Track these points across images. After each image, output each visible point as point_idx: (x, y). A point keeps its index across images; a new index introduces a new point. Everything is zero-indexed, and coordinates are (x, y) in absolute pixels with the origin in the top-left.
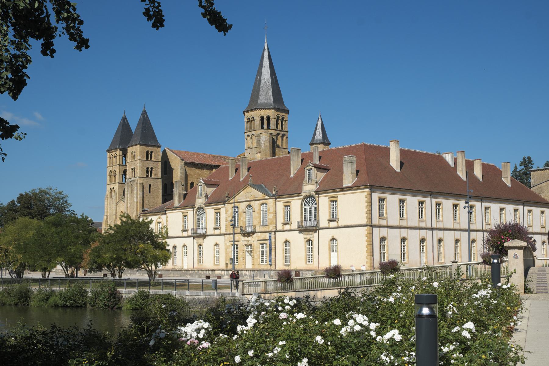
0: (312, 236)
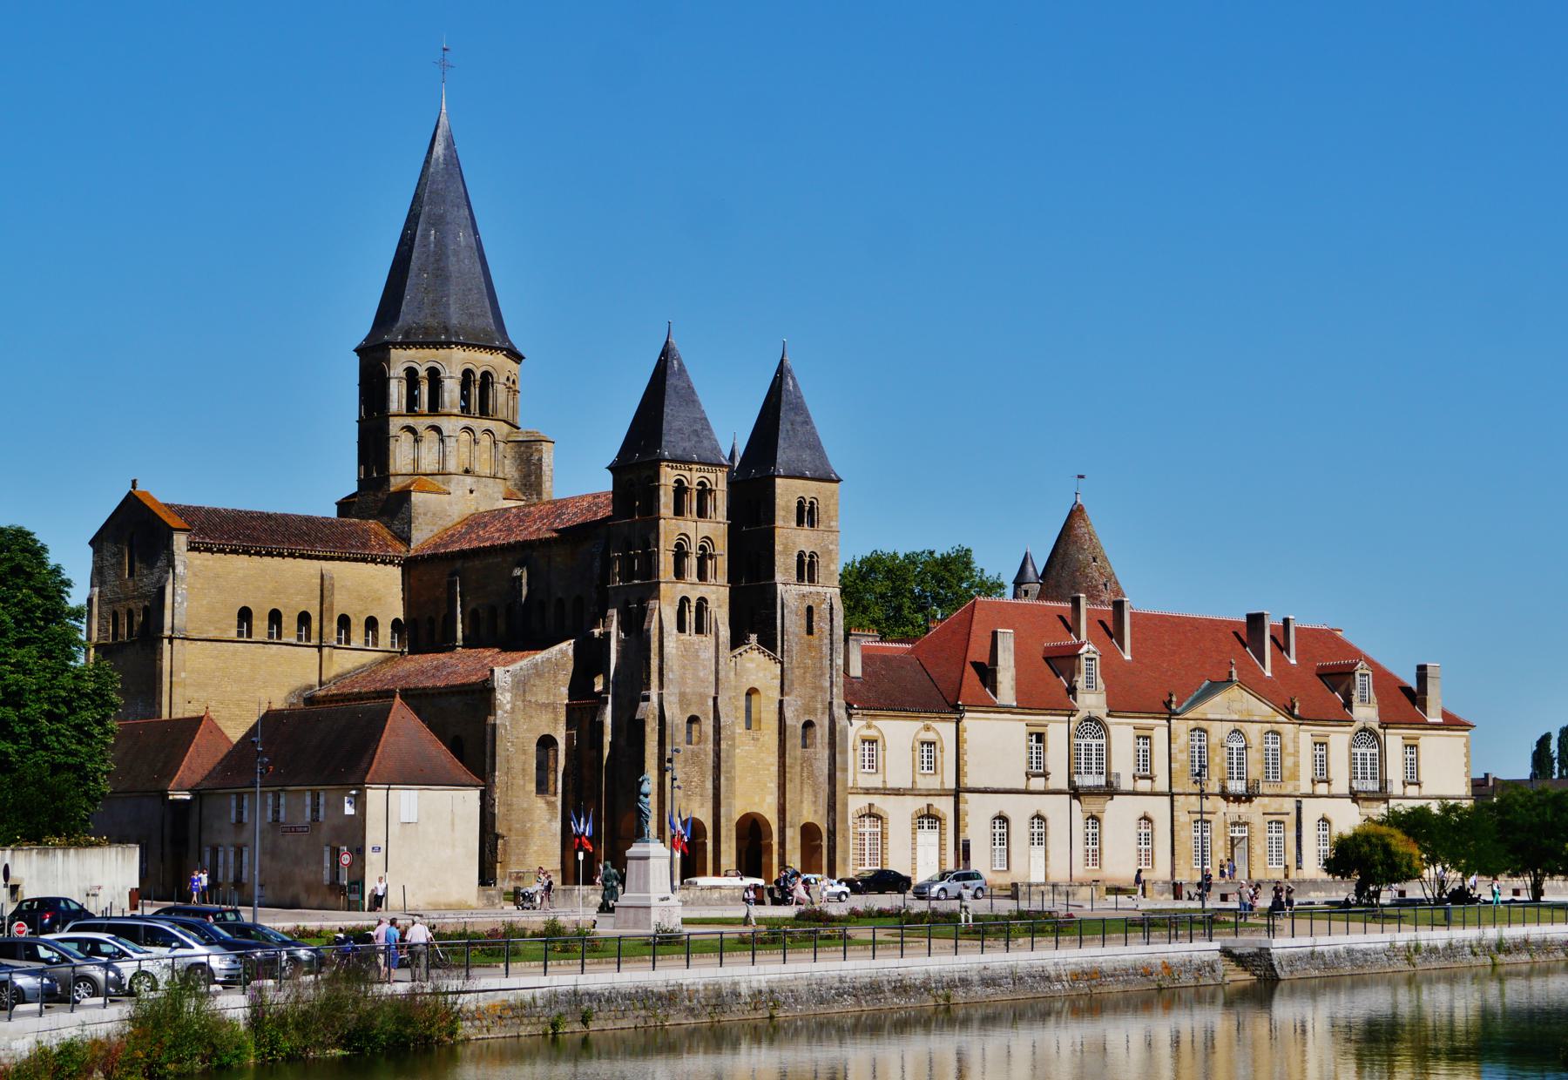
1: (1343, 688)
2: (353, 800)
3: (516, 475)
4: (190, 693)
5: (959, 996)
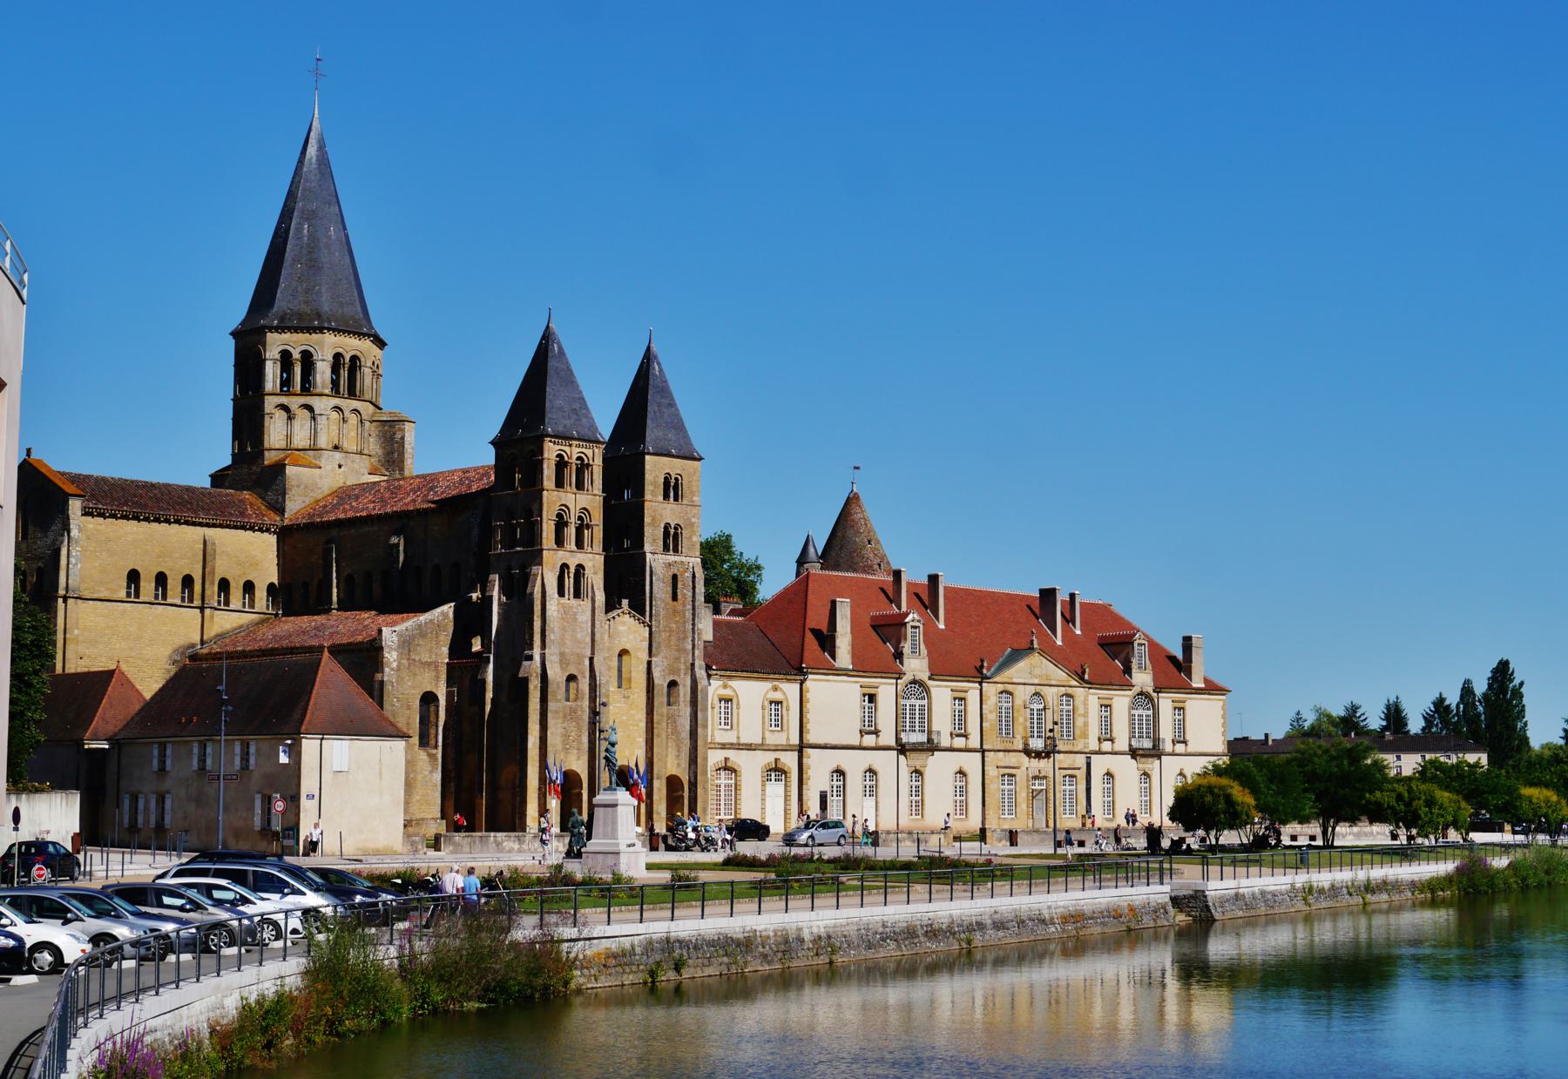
0: (1150, 766)
1: (1123, 656)
2: (287, 750)
3: (380, 452)
4: (82, 649)
5: (978, 939)
